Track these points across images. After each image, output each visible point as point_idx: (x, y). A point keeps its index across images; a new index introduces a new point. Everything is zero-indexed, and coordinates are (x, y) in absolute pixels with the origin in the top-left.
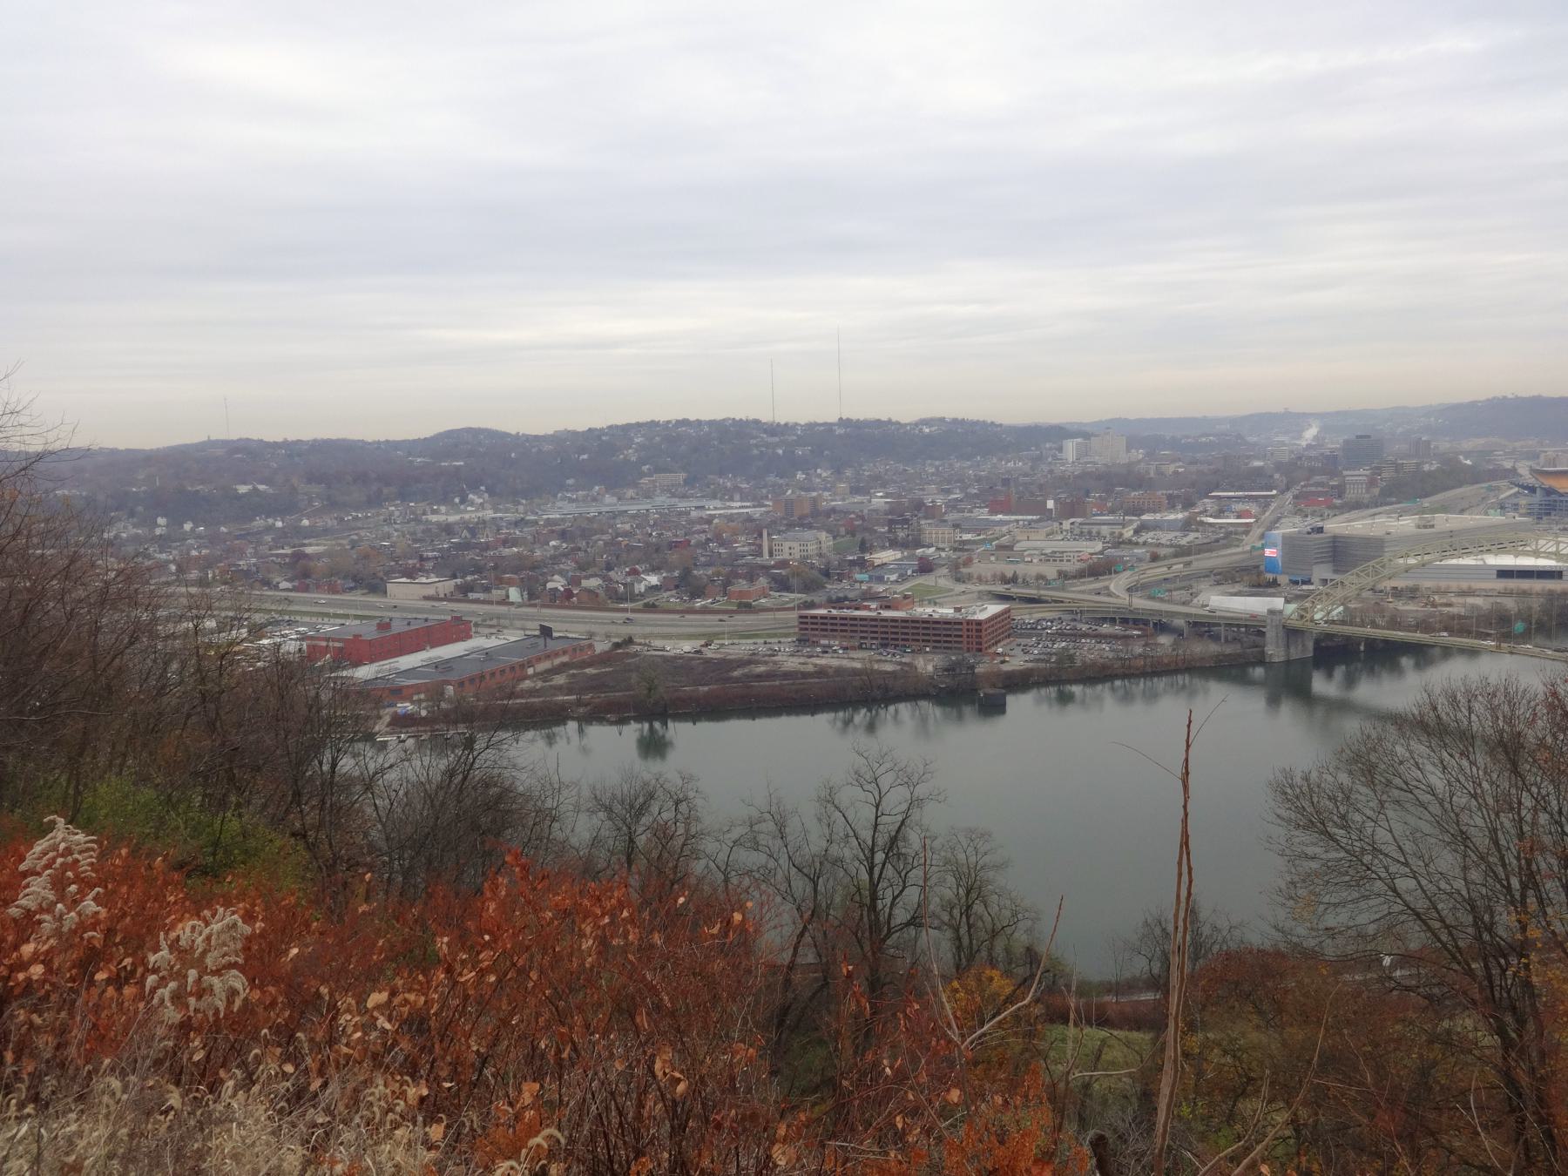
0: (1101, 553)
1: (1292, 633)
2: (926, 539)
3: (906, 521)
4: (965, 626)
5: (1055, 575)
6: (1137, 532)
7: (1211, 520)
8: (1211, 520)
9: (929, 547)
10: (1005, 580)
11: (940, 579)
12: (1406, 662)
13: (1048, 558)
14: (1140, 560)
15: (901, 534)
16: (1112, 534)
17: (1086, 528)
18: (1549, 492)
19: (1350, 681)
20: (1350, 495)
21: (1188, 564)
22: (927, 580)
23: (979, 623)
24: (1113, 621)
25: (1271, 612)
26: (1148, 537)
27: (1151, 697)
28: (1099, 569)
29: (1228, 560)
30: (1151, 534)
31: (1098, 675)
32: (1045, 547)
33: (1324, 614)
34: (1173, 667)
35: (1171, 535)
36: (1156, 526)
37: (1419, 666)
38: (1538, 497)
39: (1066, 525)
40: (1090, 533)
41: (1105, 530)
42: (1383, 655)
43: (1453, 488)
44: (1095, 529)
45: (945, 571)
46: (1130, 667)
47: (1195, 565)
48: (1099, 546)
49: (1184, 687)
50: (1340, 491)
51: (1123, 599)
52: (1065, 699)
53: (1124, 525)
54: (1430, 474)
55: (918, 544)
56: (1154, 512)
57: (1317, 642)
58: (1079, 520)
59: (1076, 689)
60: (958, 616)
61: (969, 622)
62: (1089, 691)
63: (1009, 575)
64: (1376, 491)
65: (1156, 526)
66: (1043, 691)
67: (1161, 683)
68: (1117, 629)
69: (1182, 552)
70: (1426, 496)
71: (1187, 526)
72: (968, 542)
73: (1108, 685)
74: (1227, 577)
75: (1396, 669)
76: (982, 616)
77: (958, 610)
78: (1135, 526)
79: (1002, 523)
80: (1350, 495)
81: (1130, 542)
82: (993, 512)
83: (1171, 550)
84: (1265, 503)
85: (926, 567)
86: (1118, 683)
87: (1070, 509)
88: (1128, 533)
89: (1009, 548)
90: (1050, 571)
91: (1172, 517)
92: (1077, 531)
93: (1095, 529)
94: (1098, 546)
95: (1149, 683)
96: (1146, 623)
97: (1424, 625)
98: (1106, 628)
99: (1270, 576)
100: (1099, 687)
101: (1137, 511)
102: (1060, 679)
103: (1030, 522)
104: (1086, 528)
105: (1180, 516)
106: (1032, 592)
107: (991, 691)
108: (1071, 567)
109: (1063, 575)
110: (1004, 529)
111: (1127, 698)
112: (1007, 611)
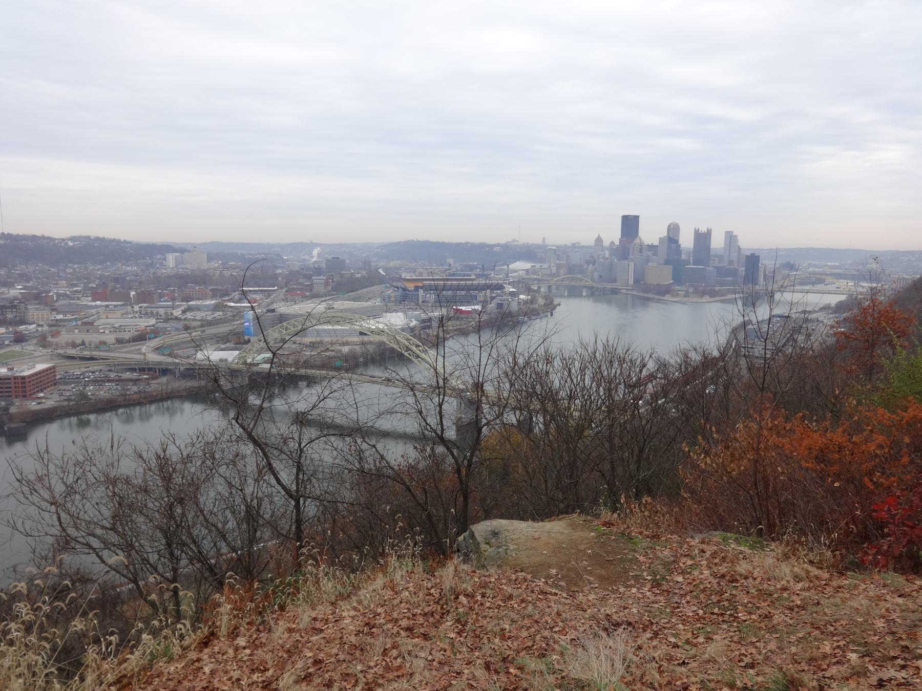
0: (153, 326)
1: (234, 373)
2: (29, 318)
3: (15, 307)
4: (13, 381)
5: (114, 341)
6: (184, 312)
7: (232, 304)
8: (232, 304)
9: (30, 324)
10: (74, 345)
11: (29, 347)
12: (302, 384)
13: (115, 329)
14: (177, 330)
15: (10, 316)
16: (166, 313)
17: (149, 310)
18: (404, 289)
19: (271, 397)
20: (316, 290)
21: (203, 331)
22: (17, 348)
23: (23, 378)
24: (133, 370)
25: (221, 360)
26: (189, 315)
27: (145, 417)
28: (141, 338)
29: (230, 328)
30: (192, 313)
31: (108, 406)
32: (114, 321)
33: (260, 359)
34: (158, 398)
35: (203, 314)
36: (198, 308)
37: (308, 386)
38: (400, 292)
39: (136, 308)
40: (152, 313)
41: (162, 311)
42: (290, 381)
43: (364, 287)
44: (155, 311)
45: (35, 341)
46: (129, 400)
47: (208, 332)
48: (153, 321)
49: (168, 409)
50: (311, 288)
51: (153, 357)
52: (84, 424)
53: (173, 308)
54: (358, 279)
55: (23, 322)
56: (199, 299)
57: (250, 377)
58: (145, 305)
59: (92, 417)
60: (10, 373)
61: (15, 378)
62: (100, 417)
63: (79, 342)
64: (330, 288)
65: (198, 308)
66: (66, 421)
67: (153, 407)
68: (135, 375)
69: (211, 324)
70: (352, 291)
71: (216, 308)
72: (60, 320)
73: (114, 412)
74: (222, 340)
75: (296, 386)
76: (26, 373)
77: (9, 369)
78: (183, 308)
79: (97, 307)
80: (316, 290)
81: (177, 319)
82: (94, 300)
83: (199, 323)
84: (268, 294)
85: (20, 339)
86: (121, 411)
87: (144, 297)
88: (177, 313)
89: (91, 324)
90: (110, 338)
91: (208, 302)
92: (143, 312)
93: (155, 311)
94: (153, 321)
95: (143, 409)
96: (150, 369)
97: (307, 364)
98: (128, 375)
99: (246, 338)
100: (108, 414)
101: (187, 299)
102: (81, 410)
103: (116, 306)
104: (149, 310)
105: (213, 302)
106: (87, 353)
107: (13, 425)
108: (127, 336)
109: (119, 341)
110: (94, 311)
111: (129, 420)
112: (54, 367)
